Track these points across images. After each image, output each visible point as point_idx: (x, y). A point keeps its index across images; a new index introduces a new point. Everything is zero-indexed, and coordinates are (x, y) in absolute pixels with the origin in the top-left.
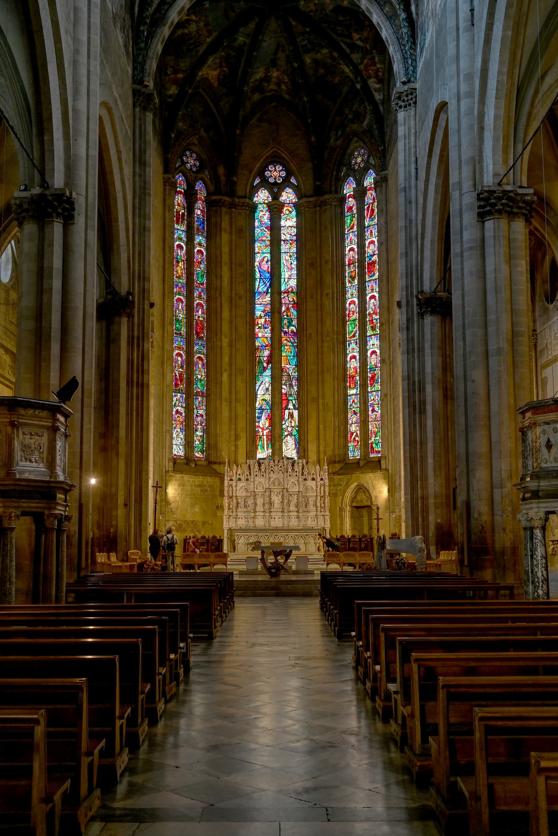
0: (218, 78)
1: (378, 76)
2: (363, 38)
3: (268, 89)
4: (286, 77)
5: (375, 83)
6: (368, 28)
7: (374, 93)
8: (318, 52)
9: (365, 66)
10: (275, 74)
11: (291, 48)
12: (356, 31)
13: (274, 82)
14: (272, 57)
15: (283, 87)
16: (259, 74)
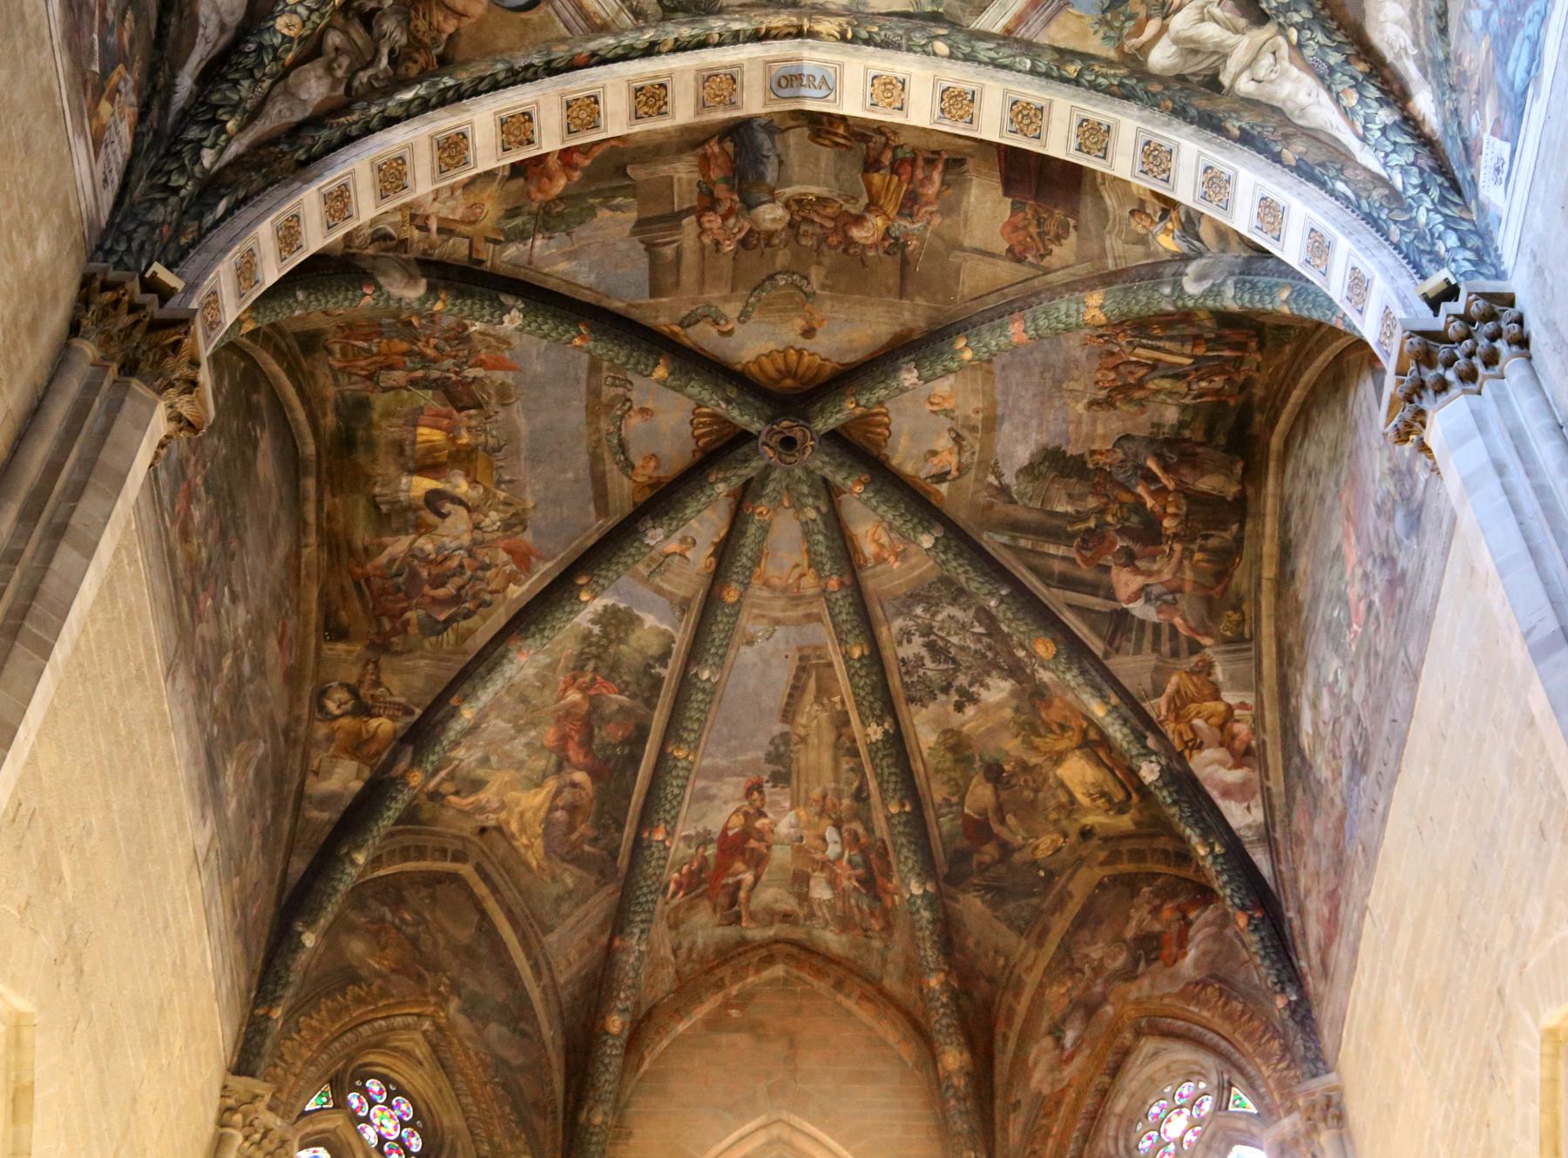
0: (548, 823)
1: (1233, 737)
2: (1156, 590)
3: (753, 906)
4: (831, 834)
5: (1222, 763)
6: (1177, 547)
7: (1223, 804)
8: (967, 698)
9: (1171, 701)
10: (784, 827)
11: (856, 653)
12: (1129, 559)
13: (782, 868)
14: (778, 728)
15: (821, 891)
16: (723, 814)
